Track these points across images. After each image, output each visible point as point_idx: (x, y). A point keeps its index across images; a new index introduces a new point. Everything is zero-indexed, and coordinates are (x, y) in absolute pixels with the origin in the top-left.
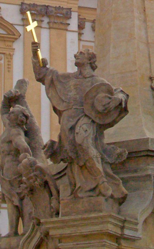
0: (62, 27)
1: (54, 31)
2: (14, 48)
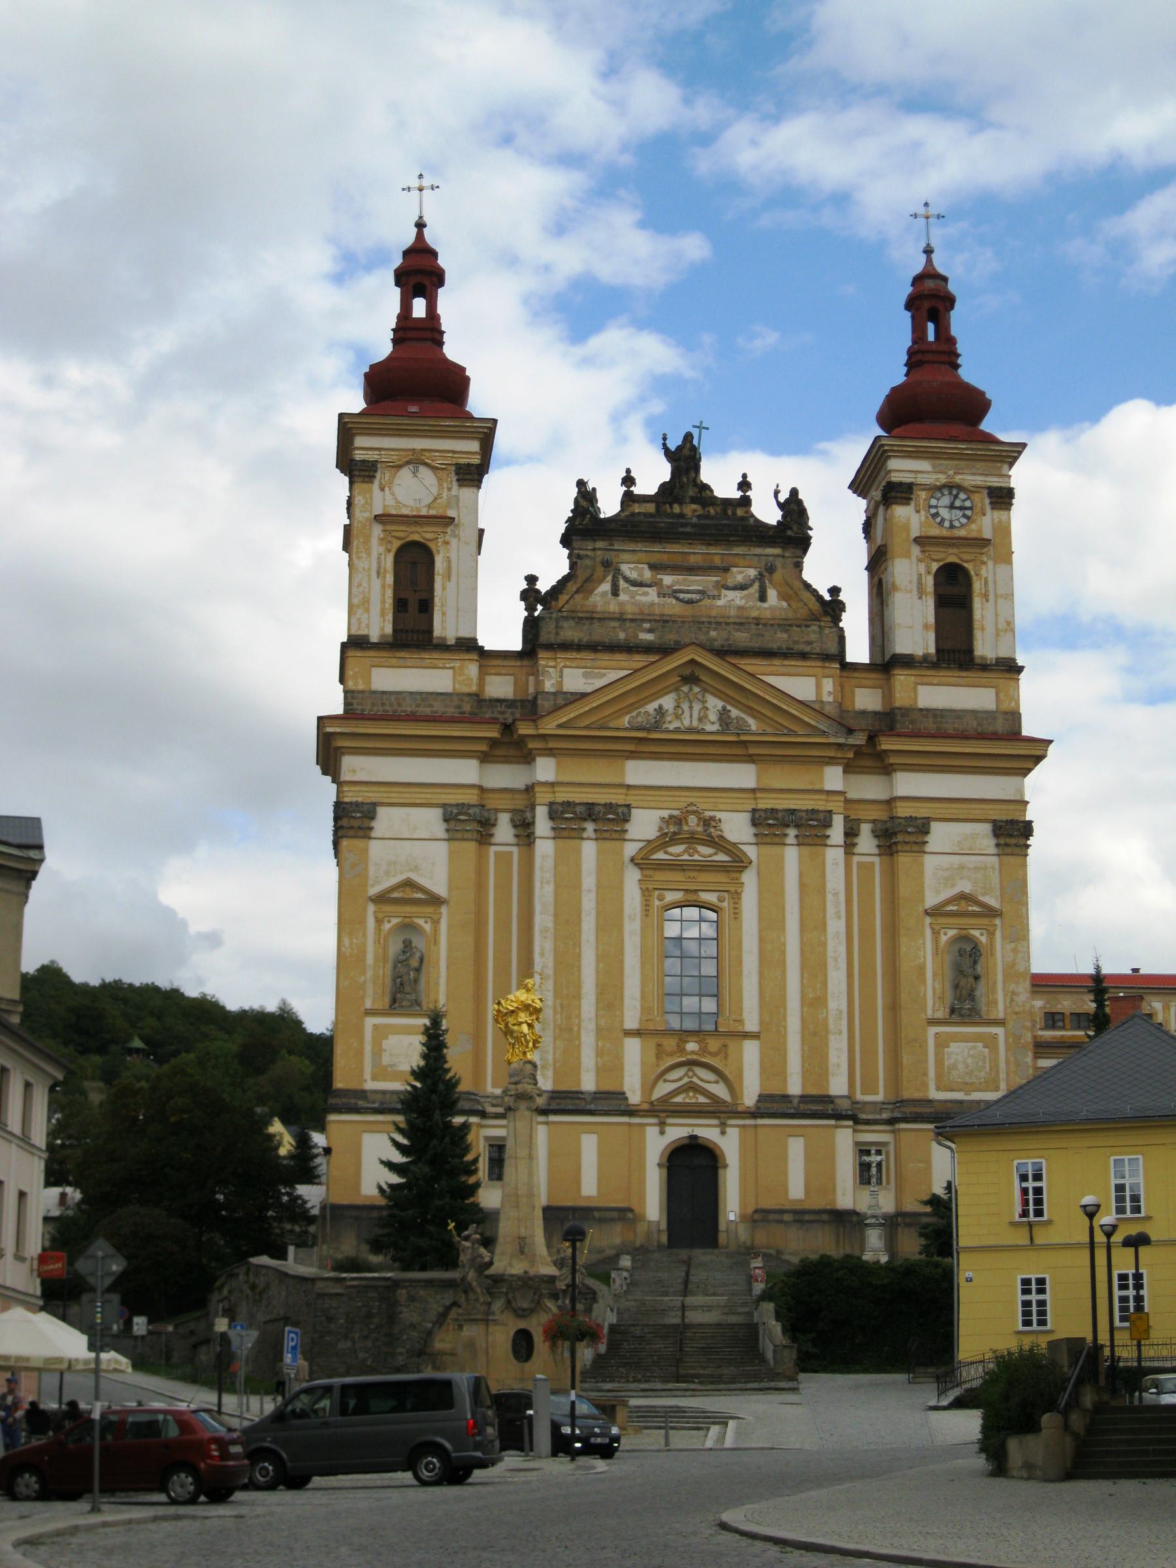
0: (819, 841)
1: (806, 850)
2: (743, 881)
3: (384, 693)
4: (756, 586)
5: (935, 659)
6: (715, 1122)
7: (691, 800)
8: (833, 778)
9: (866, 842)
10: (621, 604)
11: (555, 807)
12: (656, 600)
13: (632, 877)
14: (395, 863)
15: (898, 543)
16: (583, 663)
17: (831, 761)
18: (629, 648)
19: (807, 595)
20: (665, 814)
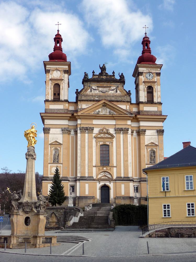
2: (113, 140)
3: (52, 109)
4: (116, 90)
5: (147, 102)
6: (109, 182)
7: (104, 126)
8: (129, 122)
9: (135, 134)
10: (92, 93)
11: (81, 128)
12: (98, 92)
13: (94, 140)
14: (54, 138)
15: (140, 82)
16: (86, 103)
17: (129, 119)
18: (94, 101)
19: (124, 91)
20: (100, 129)
